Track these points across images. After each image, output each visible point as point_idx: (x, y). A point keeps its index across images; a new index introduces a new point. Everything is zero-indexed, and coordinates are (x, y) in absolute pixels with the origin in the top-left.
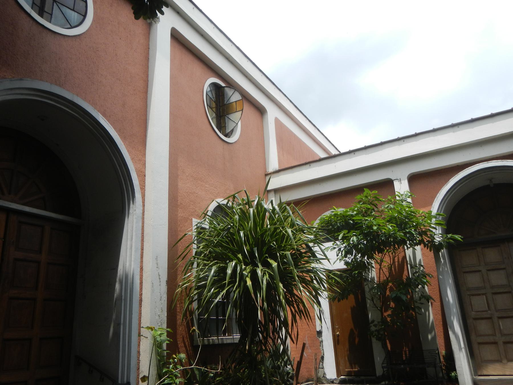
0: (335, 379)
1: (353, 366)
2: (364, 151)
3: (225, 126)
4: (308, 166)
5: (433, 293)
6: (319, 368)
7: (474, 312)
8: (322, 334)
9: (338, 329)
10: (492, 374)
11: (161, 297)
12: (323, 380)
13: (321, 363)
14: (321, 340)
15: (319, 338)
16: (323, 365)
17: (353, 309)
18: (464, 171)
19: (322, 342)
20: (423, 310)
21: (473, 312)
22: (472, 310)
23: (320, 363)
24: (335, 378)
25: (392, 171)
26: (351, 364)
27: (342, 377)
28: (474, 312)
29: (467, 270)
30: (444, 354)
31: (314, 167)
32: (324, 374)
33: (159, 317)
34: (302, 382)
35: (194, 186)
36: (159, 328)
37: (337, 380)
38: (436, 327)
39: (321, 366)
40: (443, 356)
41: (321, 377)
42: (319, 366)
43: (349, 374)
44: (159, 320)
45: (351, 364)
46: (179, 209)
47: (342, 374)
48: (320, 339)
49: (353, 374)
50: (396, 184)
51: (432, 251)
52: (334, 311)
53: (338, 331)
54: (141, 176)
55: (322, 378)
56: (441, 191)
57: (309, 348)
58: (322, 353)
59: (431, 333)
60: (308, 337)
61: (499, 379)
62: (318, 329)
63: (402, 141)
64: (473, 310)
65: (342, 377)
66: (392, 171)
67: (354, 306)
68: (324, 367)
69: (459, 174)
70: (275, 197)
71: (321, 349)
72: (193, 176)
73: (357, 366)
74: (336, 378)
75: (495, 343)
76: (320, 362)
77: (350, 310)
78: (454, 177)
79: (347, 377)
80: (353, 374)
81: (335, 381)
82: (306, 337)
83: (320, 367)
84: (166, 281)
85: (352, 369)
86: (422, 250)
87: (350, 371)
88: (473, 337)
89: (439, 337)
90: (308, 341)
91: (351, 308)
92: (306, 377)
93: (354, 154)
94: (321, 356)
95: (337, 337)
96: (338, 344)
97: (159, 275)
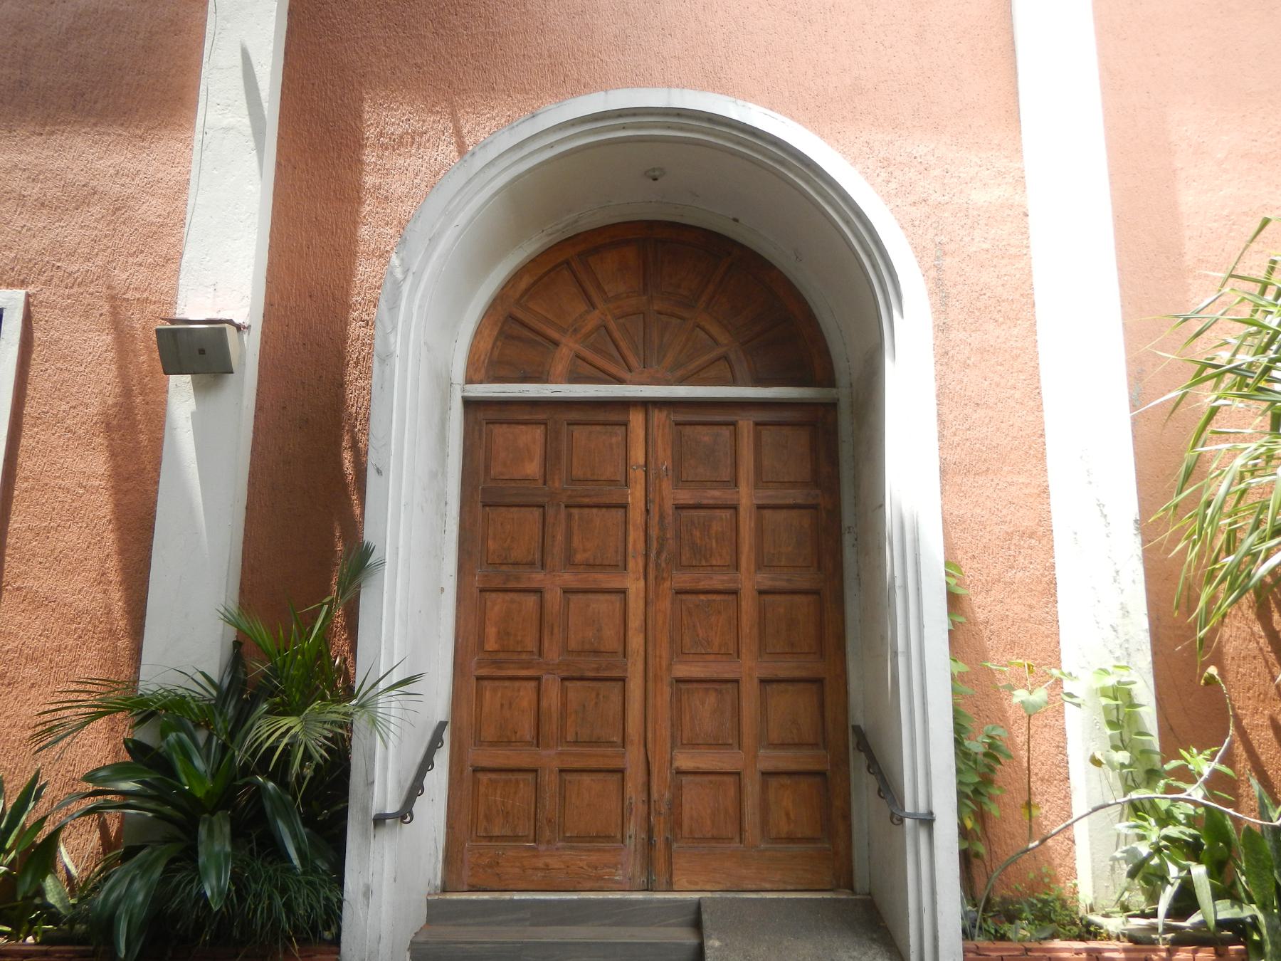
11: (1117, 572)
33: (1115, 631)
36: (1115, 666)
44: (1118, 641)
46: (1190, 281)
54: (1010, 219)
84: (1136, 521)
97: (1099, 505)
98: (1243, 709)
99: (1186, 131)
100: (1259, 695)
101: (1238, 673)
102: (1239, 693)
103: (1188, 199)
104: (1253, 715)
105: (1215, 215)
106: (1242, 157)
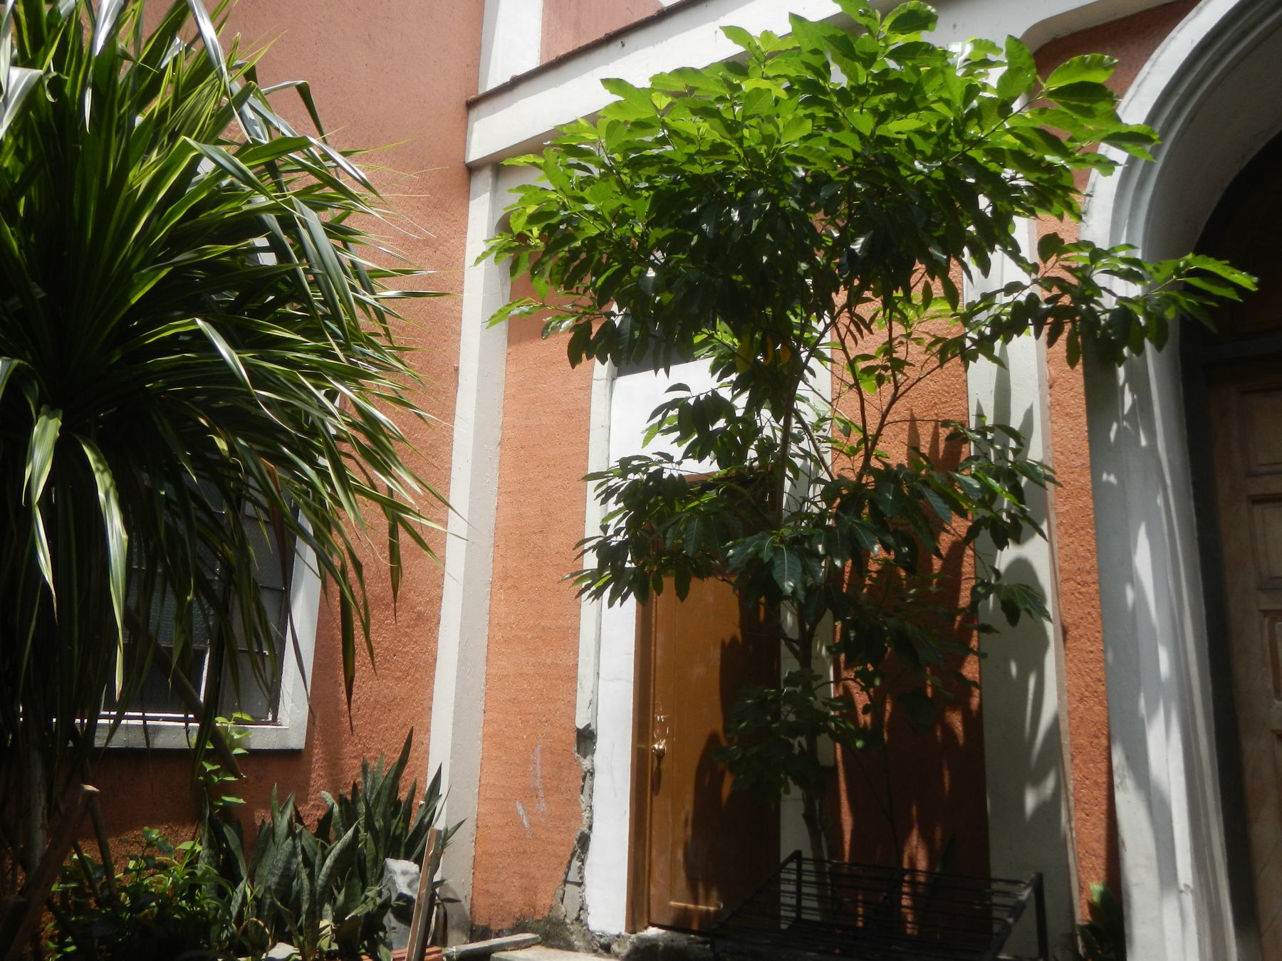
0: (618, 936)
1: (701, 890)
4: (614, 48)
5: (1080, 593)
6: (566, 882)
8: (594, 744)
9: (663, 725)
12: (572, 933)
13: (576, 863)
14: (589, 767)
15: (582, 759)
16: (581, 869)
17: (730, 651)
19: (592, 774)
20: (1014, 669)
23: (570, 862)
24: (617, 933)
26: (692, 882)
27: (652, 932)
30: (1096, 898)
31: (636, 50)
32: (581, 909)
34: (499, 927)
37: (625, 942)
38: (1077, 761)
39: (573, 876)
40: (1092, 906)
41: (568, 921)
42: (567, 874)
43: (680, 924)
45: (697, 879)
47: (654, 920)
48: (586, 763)
49: (695, 927)
51: (1079, 367)
52: (659, 654)
53: (663, 736)
55: (572, 924)
56: (1162, 52)
57: (541, 793)
58: (585, 821)
59: (1037, 780)
60: (542, 751)
62: (580, 725)
65: (652, 932)
66: (955, 26)
67: (734, 639)
68: (587, 881)
70: (495, 190)
71: (583, 806)
73: (714, 894)
74: (624, 933)
76: (572, 855)
77: (715, 654)
79: (669, 933)
80: (695, 927)
81: (615, 947)
83: (570, 878)
85: (696, 903)
86: (1051, 387)
87: (686, 909)
89: (1083, 810)
90: (542, 765)
91: (723, 644)
92: (517, 910)
94: (579, 833)
95: (656, 759)
96: (656, 788)
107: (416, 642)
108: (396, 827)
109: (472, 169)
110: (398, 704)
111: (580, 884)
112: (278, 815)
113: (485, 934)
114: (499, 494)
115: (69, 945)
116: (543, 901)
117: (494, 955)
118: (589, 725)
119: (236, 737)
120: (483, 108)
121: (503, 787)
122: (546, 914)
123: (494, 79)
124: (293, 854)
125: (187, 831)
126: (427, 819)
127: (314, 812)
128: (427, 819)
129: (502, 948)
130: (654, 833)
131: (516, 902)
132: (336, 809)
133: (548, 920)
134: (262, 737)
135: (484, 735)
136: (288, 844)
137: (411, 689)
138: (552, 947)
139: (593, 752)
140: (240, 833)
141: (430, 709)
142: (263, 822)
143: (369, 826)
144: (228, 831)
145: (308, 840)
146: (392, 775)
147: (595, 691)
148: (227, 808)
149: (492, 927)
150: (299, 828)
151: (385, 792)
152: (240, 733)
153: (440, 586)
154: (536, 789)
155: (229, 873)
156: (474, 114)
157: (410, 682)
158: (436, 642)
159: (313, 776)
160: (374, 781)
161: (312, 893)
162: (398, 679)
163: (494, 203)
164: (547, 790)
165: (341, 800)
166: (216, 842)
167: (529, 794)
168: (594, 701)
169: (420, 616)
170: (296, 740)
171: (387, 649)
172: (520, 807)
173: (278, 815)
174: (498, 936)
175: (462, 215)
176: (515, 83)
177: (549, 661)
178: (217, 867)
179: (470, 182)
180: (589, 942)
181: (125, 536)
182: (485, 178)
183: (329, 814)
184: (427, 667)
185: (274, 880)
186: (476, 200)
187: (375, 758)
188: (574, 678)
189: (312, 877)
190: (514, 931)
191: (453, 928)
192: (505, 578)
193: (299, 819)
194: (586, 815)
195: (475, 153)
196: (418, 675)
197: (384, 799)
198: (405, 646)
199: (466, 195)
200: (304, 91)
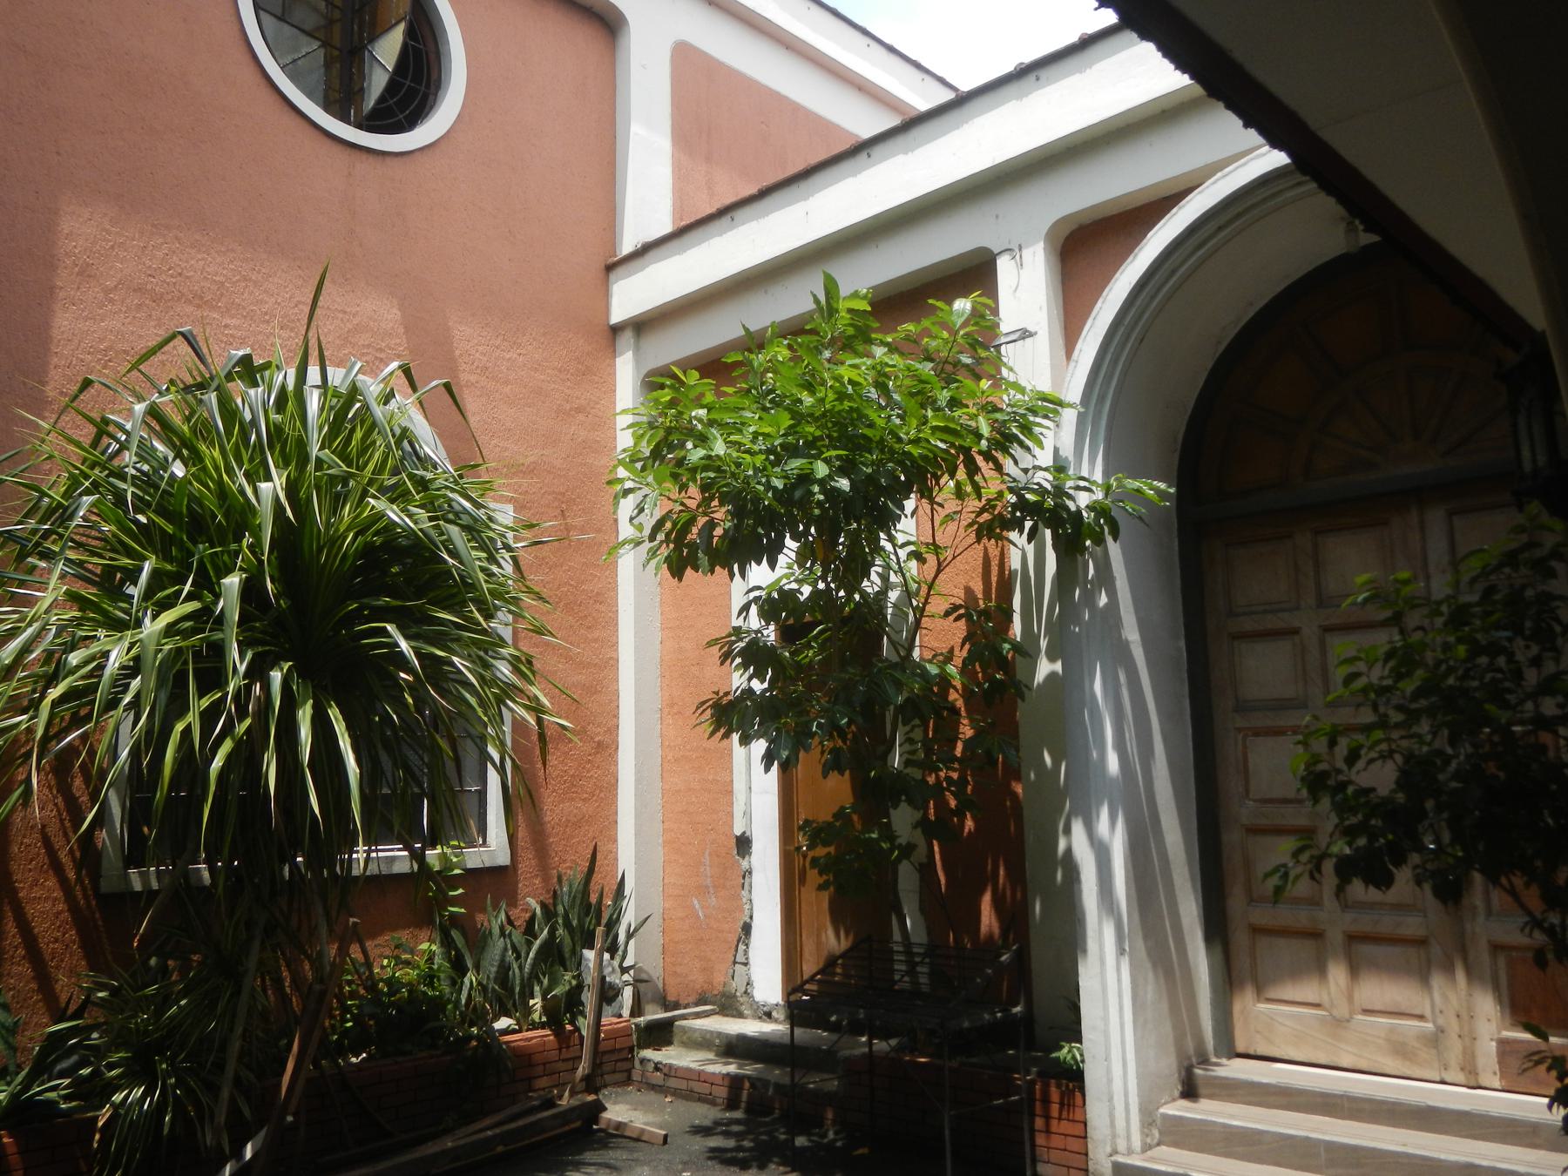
2: (900, 141)
3: (362, 90)
4: (725, 220)
6: (735, 963)
7: (1255, 801)
10: (1286, 1058)
13: (742, 947)
15: (741, 860)
16: (746, 952)
18: (1208, 187)
19: (750, 873)
21: (1250, 800)
22: (1247, 791)
23: (737, 946)
24: (775, 1002)
25: (997, 217)
28: (1251, 803)
29: (1248, 625)
32: (748, 984)
35: (152, 323)
39: (740, 958)
41: (738, 994)
48: (744, 864)
50: (1004, 266)
58: (747, 912)
60: (710, 854)
61: (1280, 1087)
63: (1032, 77)
64: (1251, 796)
66: (997, 217)
68: (751, 961)
69: (1188, 202)
71: (744, 900)
72: (149, 287)
75: (1316, 935)
78: (1167, 217)
81: (774, 1014)
82: (707, 853)
83: (737, 960)
88: (1236, 902)
90: (711, 866)
93: (869, 156)
98: (20, 882)
99: (75, 247)
100: (42, 866)
101: (22, 843)
102: (20, 865)
103: (64, 322)
104: (31, 887)
105: (91, 347)
106: (135, 290)
107: (598, 767)
108: (590, 923)
109: (616, 330)
110: (587, 821)
111: (746, 964)
112: (493, 919)
113: (676, 1006)
114: (663, 629)
115: (348, 1021)
116: (719, 979)
117: (677, 1023)
118: (744, 833)
119: (455, 860)
120: (620, 271)
121: (681, 885)
122: (721, 989)
123: (627, 248)
124: (505, 949)
125: (425, 934)
126: (615, 916)
127: (523, 915)
128: (615, 916)
129: (684, 1017)
130: (803, 920)
131: (698, 980)
132: (538, 911)
133: (723, 994)
134: (475, 858)
135: (664, 842)
136: (501, 943)
137: (598, 807)
138: (727, 1016)
139: (750, 854)
140: (464, 934)
141: (616, 822)
142: (482, 925)
143: (567, 924)
144: (455, 934)
145: (518, 937)
146: (583, 882)
147: (748, 803)
148: (453, 915)
149: (681, 1002)
150: (508, 929)
151: (580, 896)
152: (456, 857)
153: (616, 716)
154: (707, 887)
155: (459, 968)
156: (612, 276)
157: (596, 801)
158: (616, 764)
159: (520, 885)
160: (570, 886)
161: (522, 979)
162: (584, 800)
163: (638, 361)
164: (714, 887)
165: (543, 905)
166: (447, 942)
167: (702, 891)
168: (748, 811)
169: (599, 744)
170: (503, 859)
171: (573, 776)
172: (696, 902)
173: (493, 919)
174: (685, 1008)
175: (610, 374)
176: (644, 251)
177: (711, 777)
178: (450, 961)
179: (614, 346)
180: (755, 1011)
181: (358, 771)
182: (627, 337)
183: (533, 916)
184: (610, 788)
185: (494, 969)
186: (622, 358)
187: (571, 868)
188: (730, 792)
189: (521, 968)
190: (697, 1005)
191: (648, 1003)
192: (672, 705)
193: (510, 922)
194: (747, 907)
195: (616, 317)
196: (602, 795)
197: (578, 902)
198: (588, 771)
199: (613, 351)
200: (447, 387)
